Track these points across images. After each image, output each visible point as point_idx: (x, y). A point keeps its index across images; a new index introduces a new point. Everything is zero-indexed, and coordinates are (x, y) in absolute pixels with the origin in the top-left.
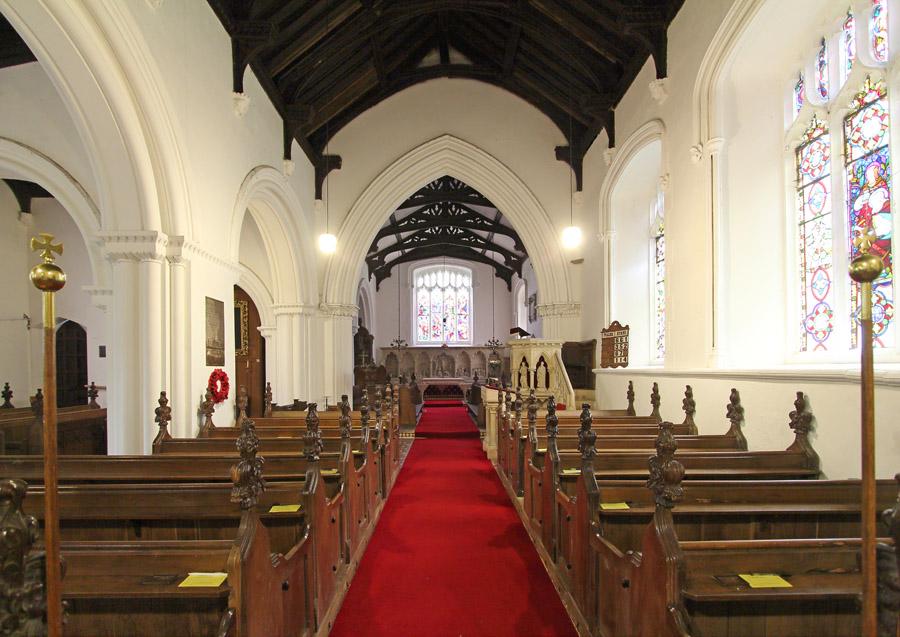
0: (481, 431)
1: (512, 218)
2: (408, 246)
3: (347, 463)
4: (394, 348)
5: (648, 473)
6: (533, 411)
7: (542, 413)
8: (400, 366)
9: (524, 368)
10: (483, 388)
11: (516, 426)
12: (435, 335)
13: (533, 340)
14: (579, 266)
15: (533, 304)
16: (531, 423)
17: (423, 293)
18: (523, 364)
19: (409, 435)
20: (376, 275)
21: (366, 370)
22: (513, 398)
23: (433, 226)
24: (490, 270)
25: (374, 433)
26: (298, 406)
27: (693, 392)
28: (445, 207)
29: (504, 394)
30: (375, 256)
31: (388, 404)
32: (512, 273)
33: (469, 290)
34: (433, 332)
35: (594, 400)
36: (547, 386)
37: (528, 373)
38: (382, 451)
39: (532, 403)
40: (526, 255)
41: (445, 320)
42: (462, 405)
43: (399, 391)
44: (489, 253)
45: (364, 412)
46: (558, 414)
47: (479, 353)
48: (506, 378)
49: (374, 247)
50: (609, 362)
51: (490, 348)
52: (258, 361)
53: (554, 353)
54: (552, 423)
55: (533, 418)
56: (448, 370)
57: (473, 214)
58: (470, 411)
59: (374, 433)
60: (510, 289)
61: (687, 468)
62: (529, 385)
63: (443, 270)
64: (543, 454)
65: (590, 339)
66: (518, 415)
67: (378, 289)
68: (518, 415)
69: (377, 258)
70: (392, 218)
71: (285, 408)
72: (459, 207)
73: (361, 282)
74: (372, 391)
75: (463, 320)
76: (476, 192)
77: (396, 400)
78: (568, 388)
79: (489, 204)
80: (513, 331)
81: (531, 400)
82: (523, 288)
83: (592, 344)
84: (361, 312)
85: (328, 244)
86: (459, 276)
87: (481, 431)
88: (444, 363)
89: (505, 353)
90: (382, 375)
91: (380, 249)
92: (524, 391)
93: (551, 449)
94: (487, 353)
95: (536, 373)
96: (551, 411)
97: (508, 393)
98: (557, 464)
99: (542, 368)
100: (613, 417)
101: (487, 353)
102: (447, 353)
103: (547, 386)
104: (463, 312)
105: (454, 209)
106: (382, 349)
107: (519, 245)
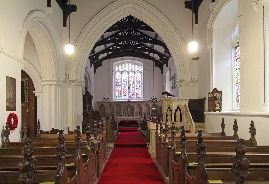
0: (148, 143)
1: (163, 37)
2: (110, 51)
3: (79, 160)
4: (103, 102)
5: (232, 164)
6: (173, 133)
7: (178, 135)
8: (106, 111)
9: (169, 112)
10: (148, 122)
11: (165, 141)
12: (124, 96)
13: (173, 98)
14: (197, 61)
15: (173, 80)
16: (173, 139)
17: (118, 74)
18: (169, 110)
19: (111, 146)
20: (94, 65)
21: (89, 113)
22: (164, 127)
23: (123, 41)
24: (152, 63)
25: (93, 145)
26: (54, 131)
27: (255, 124)
28: (129, 31)
29: (159, 125)
30: (93, 56)
31: (100, 130)
32: (163, 64)
33: (141, 73)
34: (123, 94)
35: (204, 128)
36: (181, 121)
37: (171, 114)
38: (97, 154)
39: (173, 129)
40: (170, 56)
41: (129, 88)
42: (137, 130)
43: (106, 123)
44: (151, 55)
45: (88, 134)
46: (186, 135)
47: (146, 104)
48: (160, 117)
49: (93, 51)
50: (212, 108)
51: (152, 102)
52: (33, 108)
53: (184, 104)
54: (183, 139)
55: (173, 137)
56: (131, 113)
57: (143, 35)
58: (142, 133)
59: (93, 145)
60: (162, 72)
61: (251, 162)
62: (172, 120)
63: (128, 63)
64: (179, 155)
65: (202, 97)
66: (166, 135)
67: (95, 72)
68: (166, 135)
69: (95, 57)
70: (102, 36)
71: (47, 133)
72: (136, 31)
73: (86, 69)
74: (92, 124)
75: (138, 88)
76: (145, 24)
77: (104, 128)
78: (191, 121)
79: (151, 30)
80: (164, 93)
81: (173, 128)
82: (169, 72)
83: (204, 99)
84: (86, 83)
85: (69, 49)
86: (137, 66)
87: (148, 143)
89: (160, 104)
90: (97, 115)
91: (96, 53)
92: (169, 123)
93: (183, 152)
94: (151, 104)
95: (175, 114)
96: (183, 133)
97: (161, 124)
98: (186, 160)
99: (178, 112)
100: (214, 137)
101: (151, 104)
102: (131, 105)
103: (181, 121)
104: (139, 84)
105: (134, 32)
106: (97, 102)
107: (167, 50)
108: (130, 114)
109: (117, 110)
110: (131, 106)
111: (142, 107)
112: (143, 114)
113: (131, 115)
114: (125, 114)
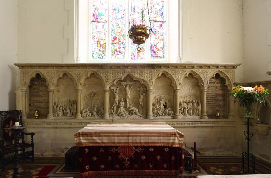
47: (191, 75)
56: (137, 105)
88: (130, 94)
108: (135, 109)
109: (90, 95)
110: (137, 81)
111: (178, 84)
112: (178, 108)
113: (136, 114)
114: (118, 107)
